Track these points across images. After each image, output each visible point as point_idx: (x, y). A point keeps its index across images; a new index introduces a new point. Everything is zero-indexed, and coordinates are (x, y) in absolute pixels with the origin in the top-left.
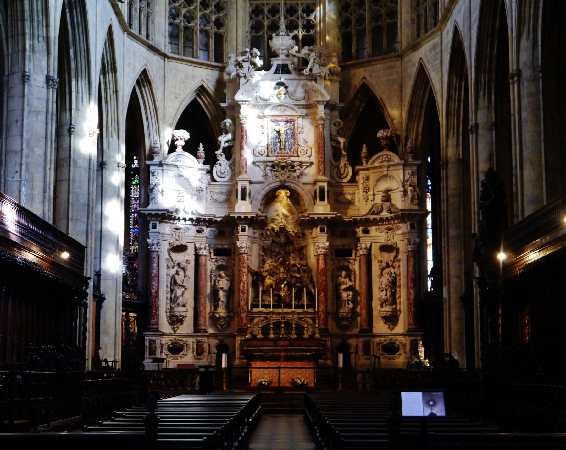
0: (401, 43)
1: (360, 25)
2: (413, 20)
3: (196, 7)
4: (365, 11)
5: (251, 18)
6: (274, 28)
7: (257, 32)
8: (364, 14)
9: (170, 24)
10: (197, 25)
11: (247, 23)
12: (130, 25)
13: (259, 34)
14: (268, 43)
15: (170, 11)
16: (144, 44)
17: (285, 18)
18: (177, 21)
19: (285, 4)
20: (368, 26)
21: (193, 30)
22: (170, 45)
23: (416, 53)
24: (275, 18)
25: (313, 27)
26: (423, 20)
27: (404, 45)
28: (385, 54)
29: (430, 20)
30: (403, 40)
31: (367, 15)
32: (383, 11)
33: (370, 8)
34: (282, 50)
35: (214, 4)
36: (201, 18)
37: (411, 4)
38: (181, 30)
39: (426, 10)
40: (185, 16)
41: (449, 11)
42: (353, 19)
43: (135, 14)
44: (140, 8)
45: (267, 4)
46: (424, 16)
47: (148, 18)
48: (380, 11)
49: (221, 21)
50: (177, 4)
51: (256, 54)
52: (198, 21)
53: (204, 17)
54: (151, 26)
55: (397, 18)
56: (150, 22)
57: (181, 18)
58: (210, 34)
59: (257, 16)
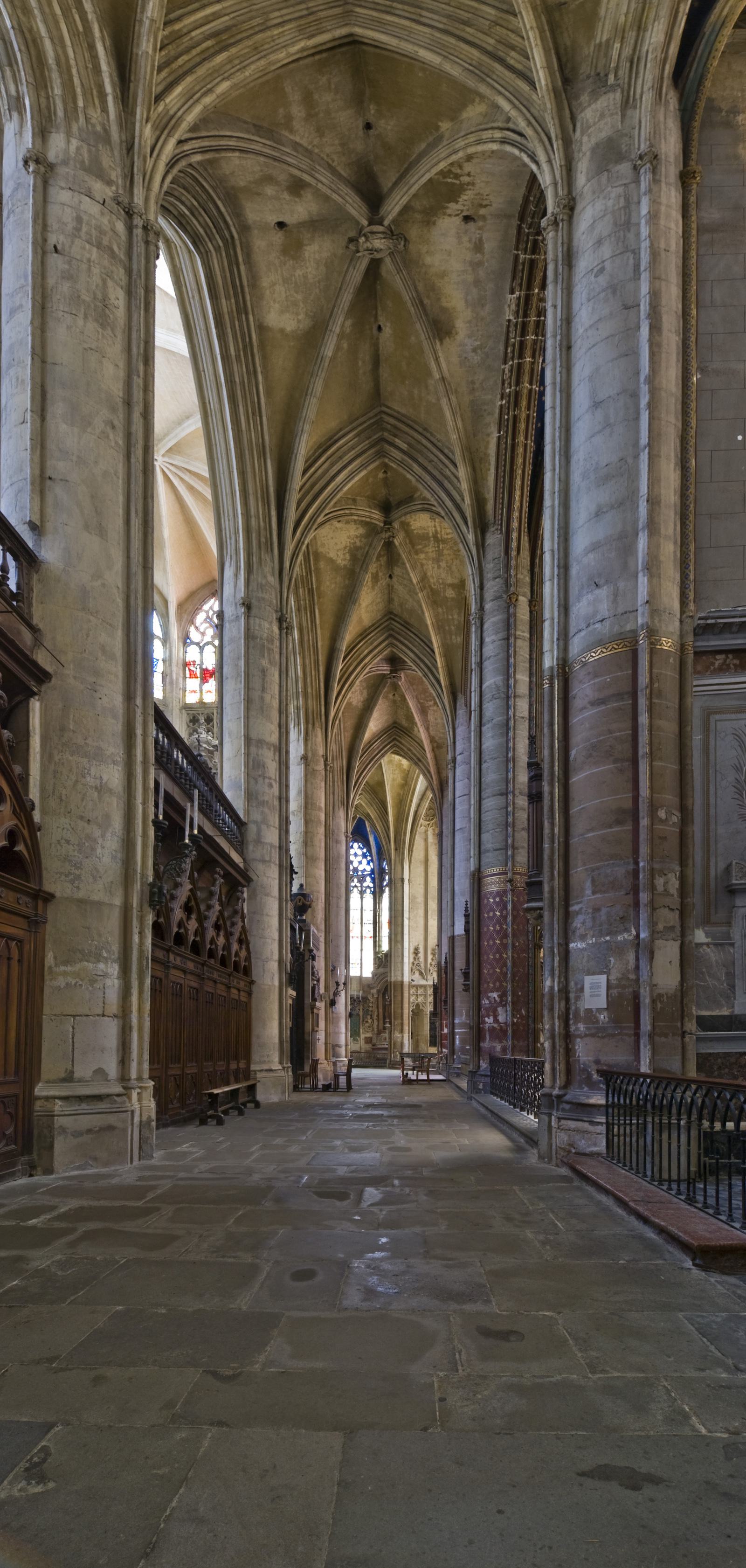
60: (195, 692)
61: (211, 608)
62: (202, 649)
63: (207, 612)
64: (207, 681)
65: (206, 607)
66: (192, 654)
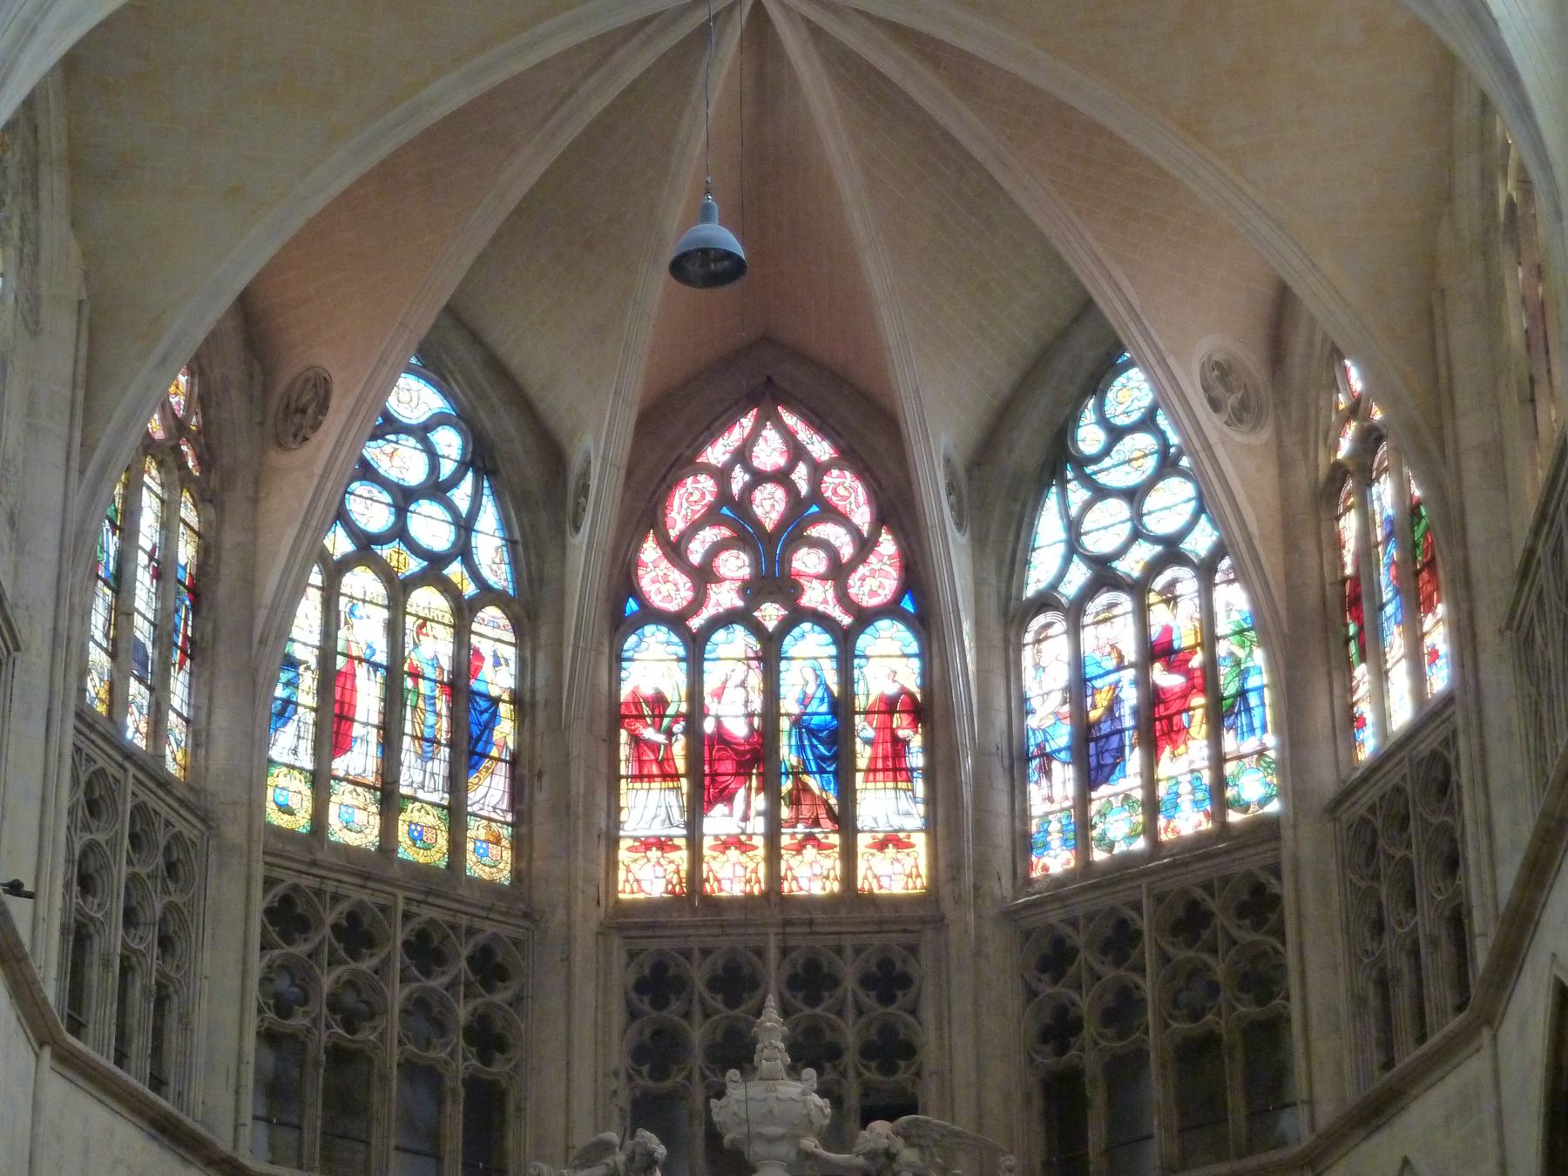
0: (1311, 1103)
1: (1121, 1035)
2: (1359, 1002)
3: (387, 960)
4: (1141, 970)
5: (633, 1015)
6: (736, 1052)
7: (660, 1073)
8: (1137, 987)
9: (269, 1037)
10: (388, 1038)
11: (615, 1039)
12: (77, 1027)
13: (668, 1084)
14: (708, 1111)
15: (265, 980)
16: (133, 1110)
17: (786, 1012)
18: (298, 1021)
19: (785, 952)
20: (1156, 1036)
21: (370, 1061)
22: (262, 1125)
23: (1379, 1139)
24: (738, 1012)
25: (909, 1050)
26: (1402, 998)
27: (1326, 1113)
28: (1240, 1156)
29: (1439, 992)
30: (1319, 1090)
31: (1149, 987)
32: (1220, 969)
33: (1165, 959)
34: (771, 1140)
35: (465, 952)
36: (404, 1011)
37: (1347, 930)
38: (316, 1063)
39: (1415, 954)
40: (334, 1005)
41: (1521, 920)
42: (1085, 1005)
43: (101, 981)
44: (123, 958)
45: (705, 952)
46: (1407, 977)
47: (161, 1002)
48: (1208, 968)
49: (499, 1026)
50: (301, 949)
51: (650, 1154)
52: (393, 1022)
53: (420, 1005)
54: (173, 1039)
55: (1287, 998)
56: (172, 1021)
57: (320, 1007)
58: (449, 1084)
59: (660, 1003)
60: (663, 844)
61: (742, 455)
62: (695, 649)
63: (721, 475)
64: (726, 797)
65: (717, 453)
66: (651, 666)
